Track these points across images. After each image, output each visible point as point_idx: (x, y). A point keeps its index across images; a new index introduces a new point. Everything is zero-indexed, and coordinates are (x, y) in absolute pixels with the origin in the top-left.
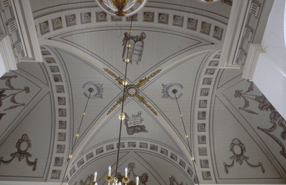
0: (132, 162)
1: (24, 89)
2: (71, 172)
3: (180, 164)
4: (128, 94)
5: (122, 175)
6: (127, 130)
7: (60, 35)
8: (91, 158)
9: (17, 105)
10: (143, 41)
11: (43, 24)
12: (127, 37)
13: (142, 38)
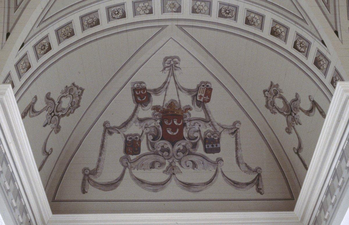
0: (173, 55)
2: (20, 67)
3: (295, 47)
5: (147, 88)
8: (68, 37)
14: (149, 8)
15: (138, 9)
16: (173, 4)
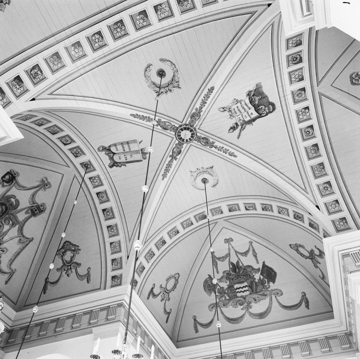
1: (229, 244)
4: (192, 139)
6: (267, 114)
7: (126, 243)
9: (251, 249)
10: (108, 147)
11: (114, 266)
12: (113, 164)
13: (105, 148)
14: (303, 110)
15: (305, 118)
16: (298, 95)
